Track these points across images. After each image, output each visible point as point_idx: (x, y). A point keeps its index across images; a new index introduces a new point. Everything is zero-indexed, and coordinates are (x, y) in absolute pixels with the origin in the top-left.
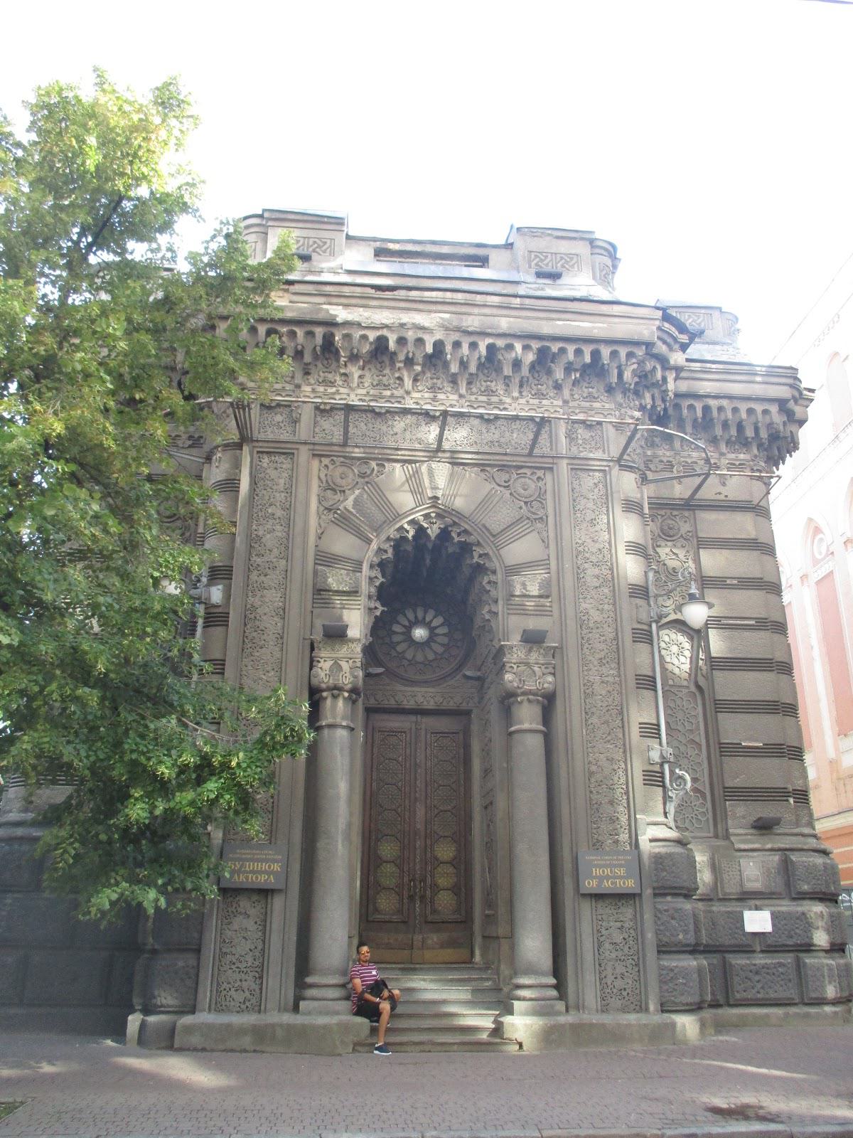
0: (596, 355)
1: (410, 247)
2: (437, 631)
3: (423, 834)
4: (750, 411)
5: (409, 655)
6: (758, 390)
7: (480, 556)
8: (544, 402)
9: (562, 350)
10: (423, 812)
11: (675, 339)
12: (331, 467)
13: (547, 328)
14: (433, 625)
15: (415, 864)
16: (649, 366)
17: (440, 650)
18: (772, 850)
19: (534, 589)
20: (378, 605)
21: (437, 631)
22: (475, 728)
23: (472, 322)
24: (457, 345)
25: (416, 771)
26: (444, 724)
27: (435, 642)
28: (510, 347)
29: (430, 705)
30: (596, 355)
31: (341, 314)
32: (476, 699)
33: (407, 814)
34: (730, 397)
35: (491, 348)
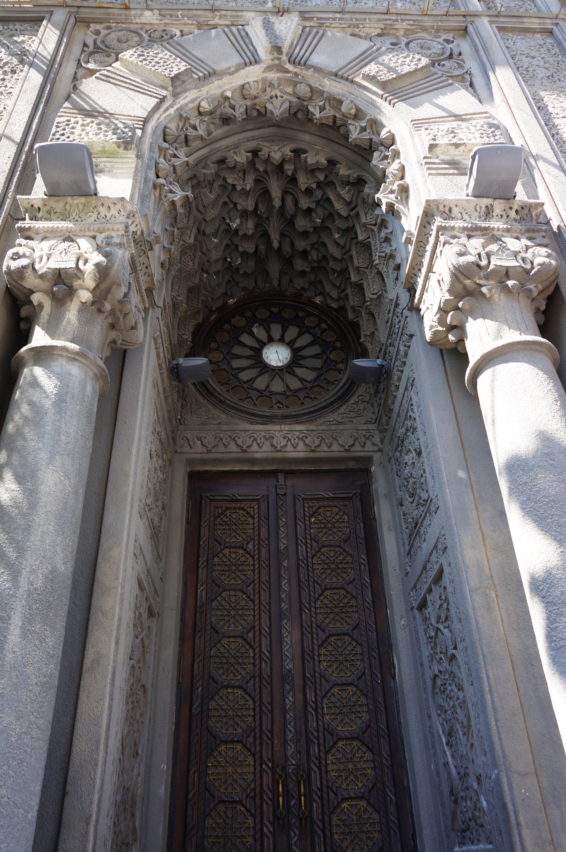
2: (304, 353)
3: (298, 681)
5: (261, 383)
7: (363, 129)
10: (297, 636)
12: (104, 32)
14: (297, 345)
15: (285, 743)
17: (309, 376)
20: (176, 188)
21: (304, 353)
22: (380, 486)
25: (279, 564)
26: (324, 488)
27: (301, 366)
29: (301, 452)
32: (377, 439)
33: (265, 642)
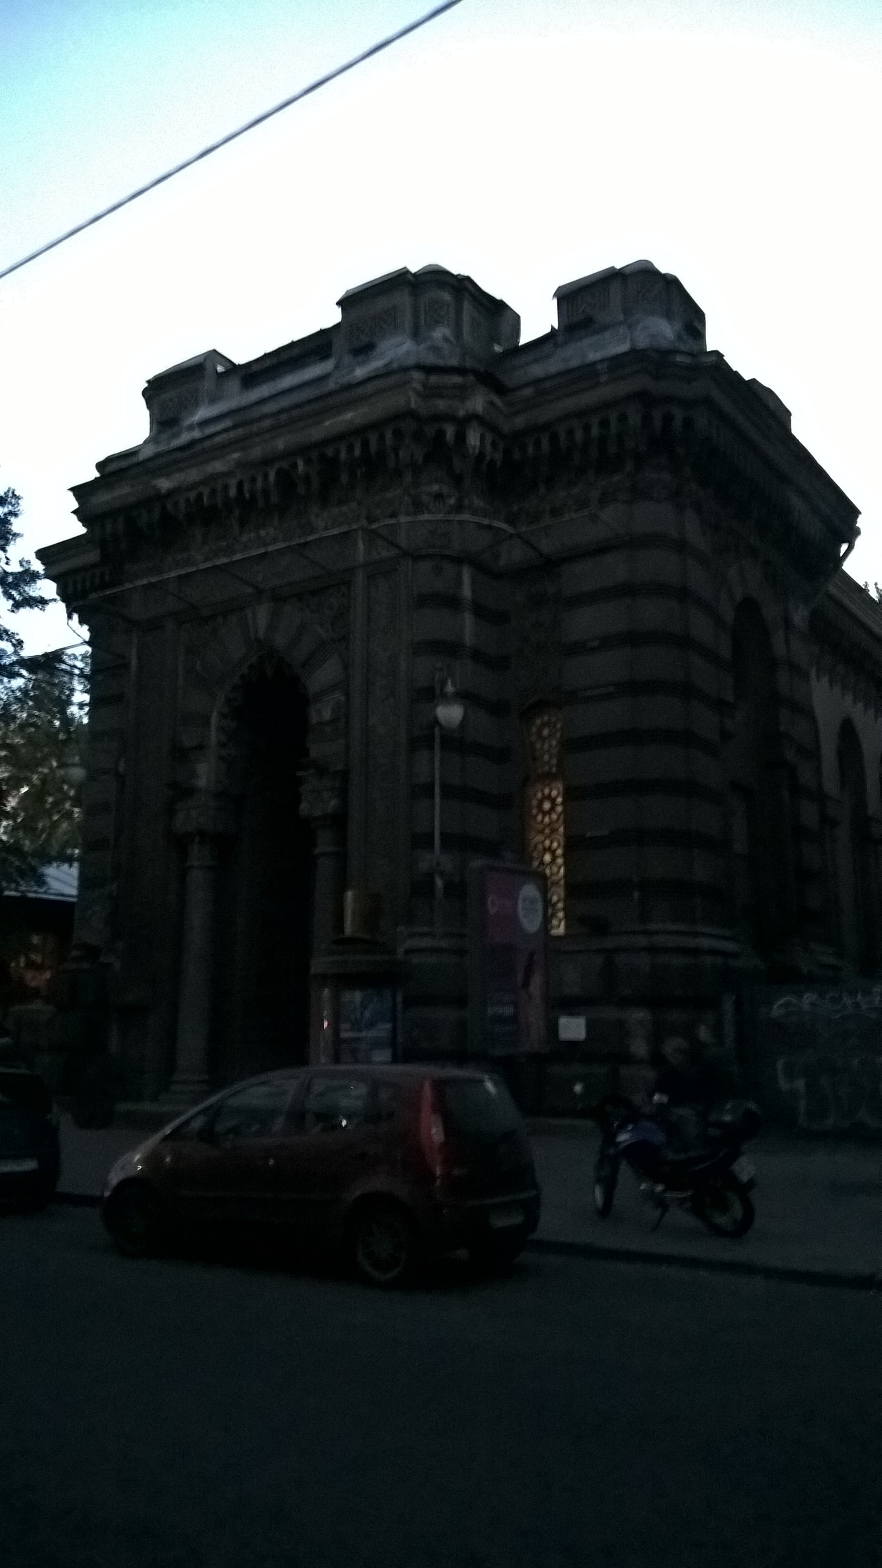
0: (365, 445)
1: (268, 363)
4: (604, 424)
6: (605, 392)
8: (345, 509)
9: (337, 451)
11: (462, 388)
13: (317, 433)
16: (430, 431)
18: (598, 951)
19: (327, 715)
23: (256, 453)
24: (253, 480)
28: (295, 466)
30: (365, 445)
31: (164, 484)
34: (581, 414)
35: (279, 472)
